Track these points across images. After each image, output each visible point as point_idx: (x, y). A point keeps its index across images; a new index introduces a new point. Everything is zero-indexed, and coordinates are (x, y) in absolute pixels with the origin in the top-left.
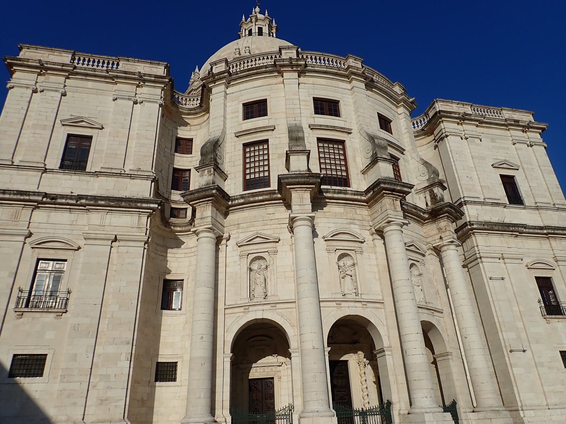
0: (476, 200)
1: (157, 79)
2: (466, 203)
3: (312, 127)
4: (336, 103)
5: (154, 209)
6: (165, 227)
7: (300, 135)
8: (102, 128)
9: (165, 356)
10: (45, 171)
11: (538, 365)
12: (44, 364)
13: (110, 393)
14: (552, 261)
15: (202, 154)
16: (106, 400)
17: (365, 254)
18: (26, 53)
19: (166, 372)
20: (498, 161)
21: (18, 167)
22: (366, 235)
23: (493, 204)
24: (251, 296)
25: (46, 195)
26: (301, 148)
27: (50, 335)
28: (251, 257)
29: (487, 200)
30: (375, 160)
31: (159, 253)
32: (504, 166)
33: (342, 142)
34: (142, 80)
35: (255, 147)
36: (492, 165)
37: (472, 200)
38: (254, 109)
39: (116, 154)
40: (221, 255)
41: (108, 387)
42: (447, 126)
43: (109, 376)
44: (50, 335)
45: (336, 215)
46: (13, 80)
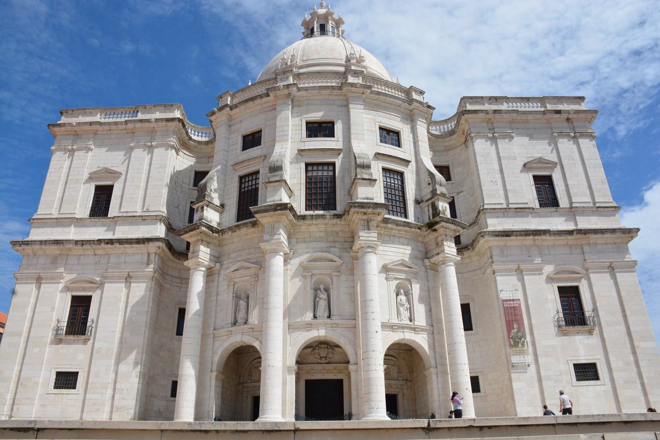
0: (497, 207)
6: (179, 259)
7: (278, 164)
11: (543, 379)
16: (121, 408)
17: (343, 277)
20: (532, 159)
24: (235, 323)
29: (511, 206)
31: (174, 284)
37: (493, 207)
38: (252, 140)
39: (132, 198)
41: (122, 398)
43: (123, 389)
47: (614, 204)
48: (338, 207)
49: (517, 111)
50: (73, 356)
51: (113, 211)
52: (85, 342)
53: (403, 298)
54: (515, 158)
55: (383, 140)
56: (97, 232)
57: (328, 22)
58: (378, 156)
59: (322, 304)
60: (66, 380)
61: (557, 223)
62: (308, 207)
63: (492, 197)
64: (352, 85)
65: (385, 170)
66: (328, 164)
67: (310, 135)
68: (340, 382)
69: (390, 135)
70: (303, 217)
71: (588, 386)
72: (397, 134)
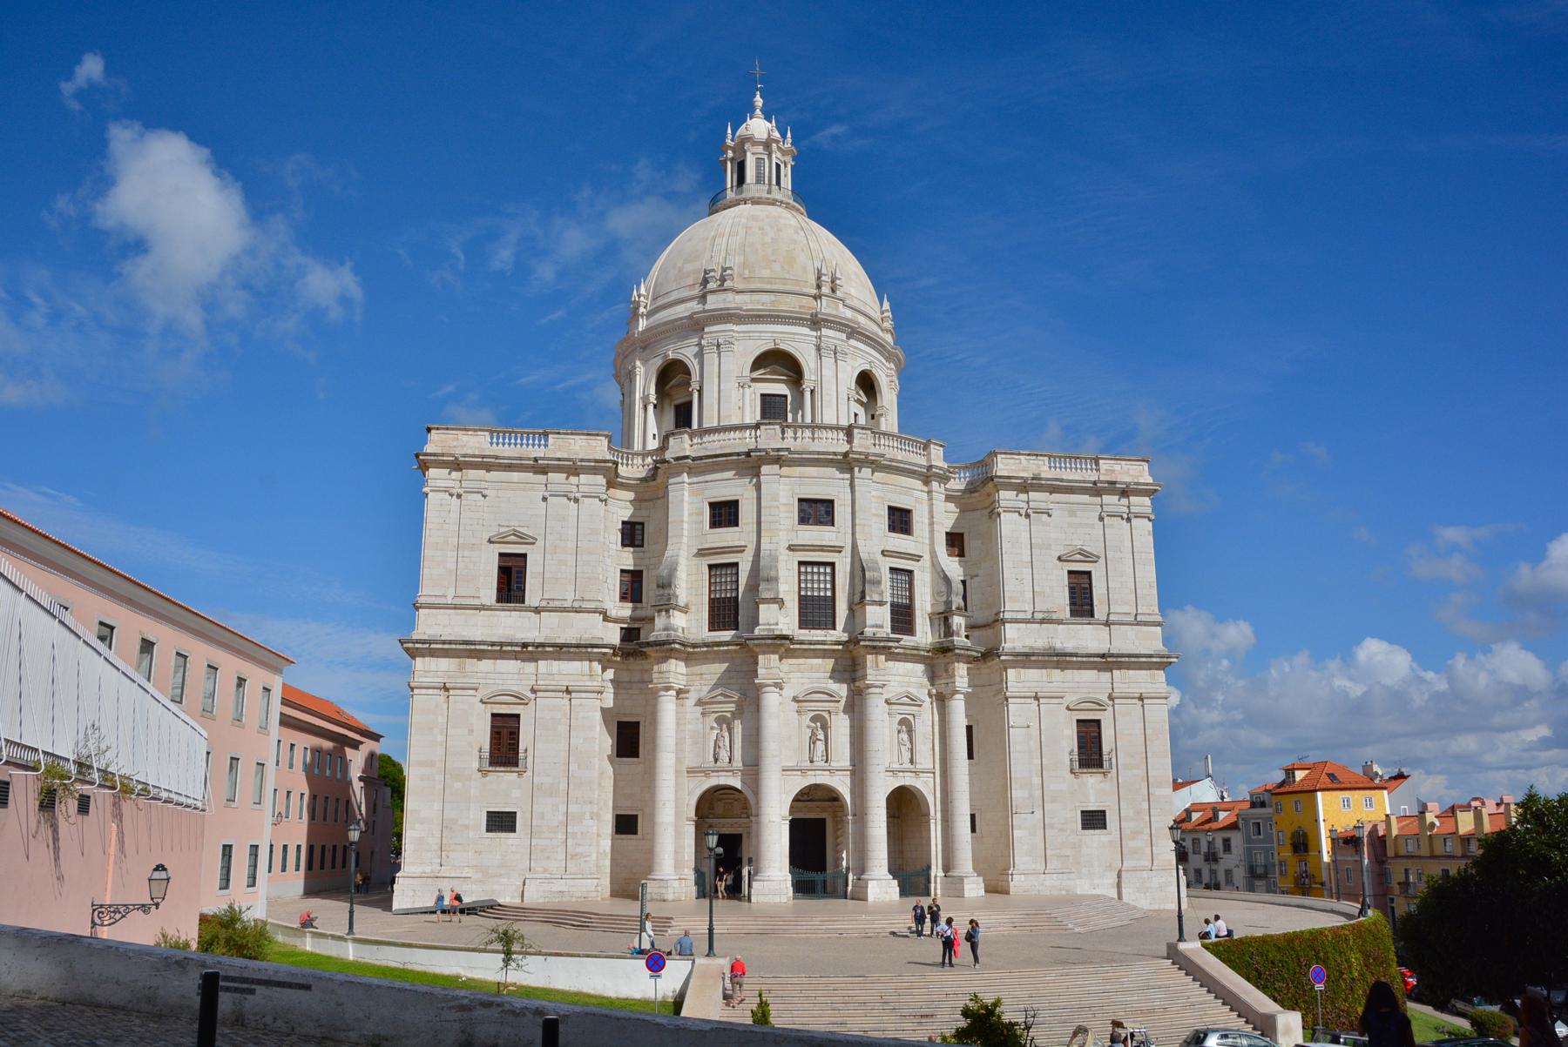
0: (1020, 616)
1: (596, 467)
3: (791, 548)
7: (773, 574)
10: (482, 608)
12: (514, 822)
13: (579, 850)
18: (437, 442)
21: (456, 607)
23: (1043, 621)
25: (493, 644)
27: (516, 793)
33: (832, 565)
35: (722, 570)
36: (1059, 559)
37: (1014, 615)
44: (516, 793)
45: (812, 669)
47: (1159, 619)
49: (1062, 480)
50: (505, 789)
51: (532, 598)
52: (520, 774)
53: (905, 736)
54: (1049, 547)
55: (893, 528)
56: (512, 625)
57: (770, 156)
59: (820, 746)
60: (501, 822)
61: (1086, 638)
62: (804, 623)
63: (1016, 599)
66: (825, 564)
67: (804, 520)
68: (824, 820)
69: (900, 520)
70: (802, 643)
71: (1095, 836)
72: (908, 512)
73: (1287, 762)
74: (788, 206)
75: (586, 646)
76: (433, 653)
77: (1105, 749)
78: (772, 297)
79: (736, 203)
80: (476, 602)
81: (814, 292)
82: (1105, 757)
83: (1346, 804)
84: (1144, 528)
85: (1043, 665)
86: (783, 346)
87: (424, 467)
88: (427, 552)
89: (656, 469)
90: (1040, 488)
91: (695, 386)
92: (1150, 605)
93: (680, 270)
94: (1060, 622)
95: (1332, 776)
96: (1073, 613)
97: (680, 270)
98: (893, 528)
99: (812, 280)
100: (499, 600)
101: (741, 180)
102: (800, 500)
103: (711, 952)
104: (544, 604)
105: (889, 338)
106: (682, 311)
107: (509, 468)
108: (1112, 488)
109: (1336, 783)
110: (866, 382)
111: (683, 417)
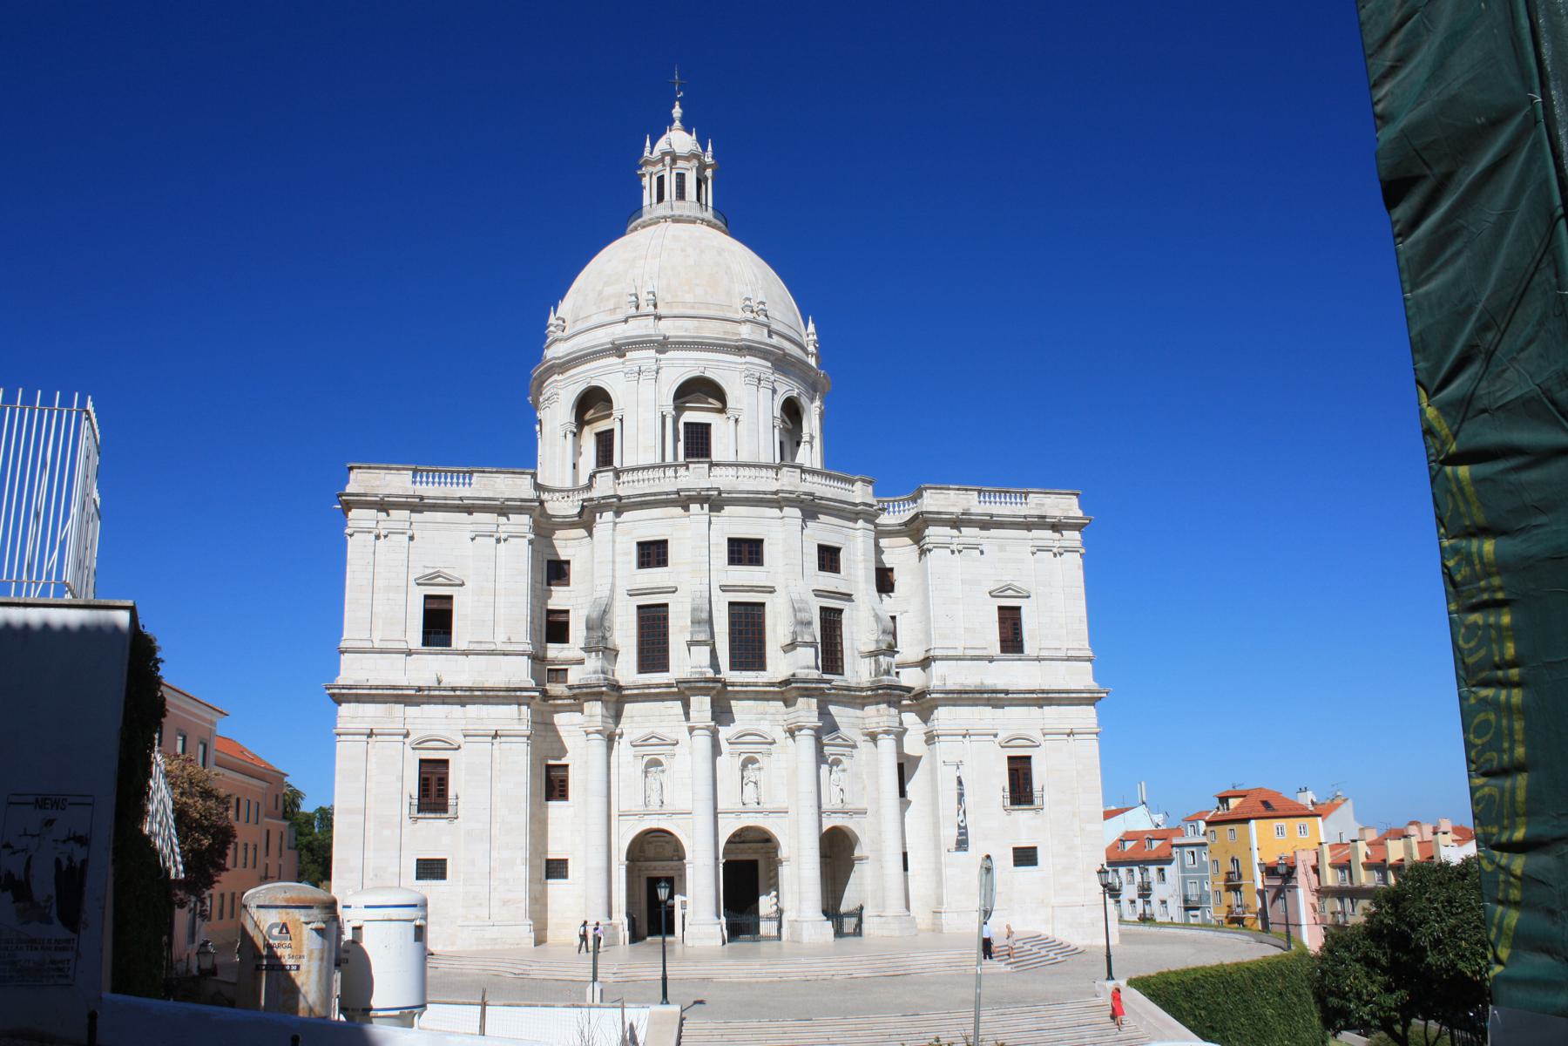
2: (935, 659)
3: (725, 589)
4: (758, 543)
5: (533, 698)
8: (462, 585)
9: (553, 854)
10: (409, 653)
14: (1037, 735)
15: (589, 628)
17: (774, 756)
18: (360, 481)
19: (556, 869)
21: (382, 651)
22: (779, 734)
23: (973, 658)
25: (420, 689)
26: (702, 637)
28: (646, 759)
30: (793, 646)
32: (1010, 593)
34: (503, 509)
38: (653, 553)
40: (614, 752)
42: (934, 533)
46: (350, 523)
47: (1090, 654)
48: (769, 667)
50: (432, 836)
55: (823, 566)
58: (819, 593)
64: (791, 492)
65: (823, 609)
69: (829, 558)
70: (733, 685)
73: (1223, 789)
74: (709, 224)
75: (515, 690)
76: (359, 699)
77: (1036, 785)
78: (695, 322)
79: (655, 221)
80: (403, 646)
81: (740, 315)
82: (1036, 793)
83: (1280, 831)
84: (1075, 561)
85: (975, 703)
86: (708, 374)
87: (348, 507)
88: (349, 595)
89: (583, 507)
90: (970, 523)
91: (616, 413)
92: (1080, 641)
93: (600, 293)
94: (991, 660)
95: (1266, 804)
96: (1004, 649)
97: (600, 293)
98: (822, 567)
99: (738, 304)
100: (426, 643)
101: (660, 198)
102: (730, 540)
103: (665, 999)
104: (472, 647)
105: (812, 361)
106: (602, 337)
107: (434, 508)
108: (1041, 523)
109: (1270, 808)
110: (792, 411)
111: (605, 443)
